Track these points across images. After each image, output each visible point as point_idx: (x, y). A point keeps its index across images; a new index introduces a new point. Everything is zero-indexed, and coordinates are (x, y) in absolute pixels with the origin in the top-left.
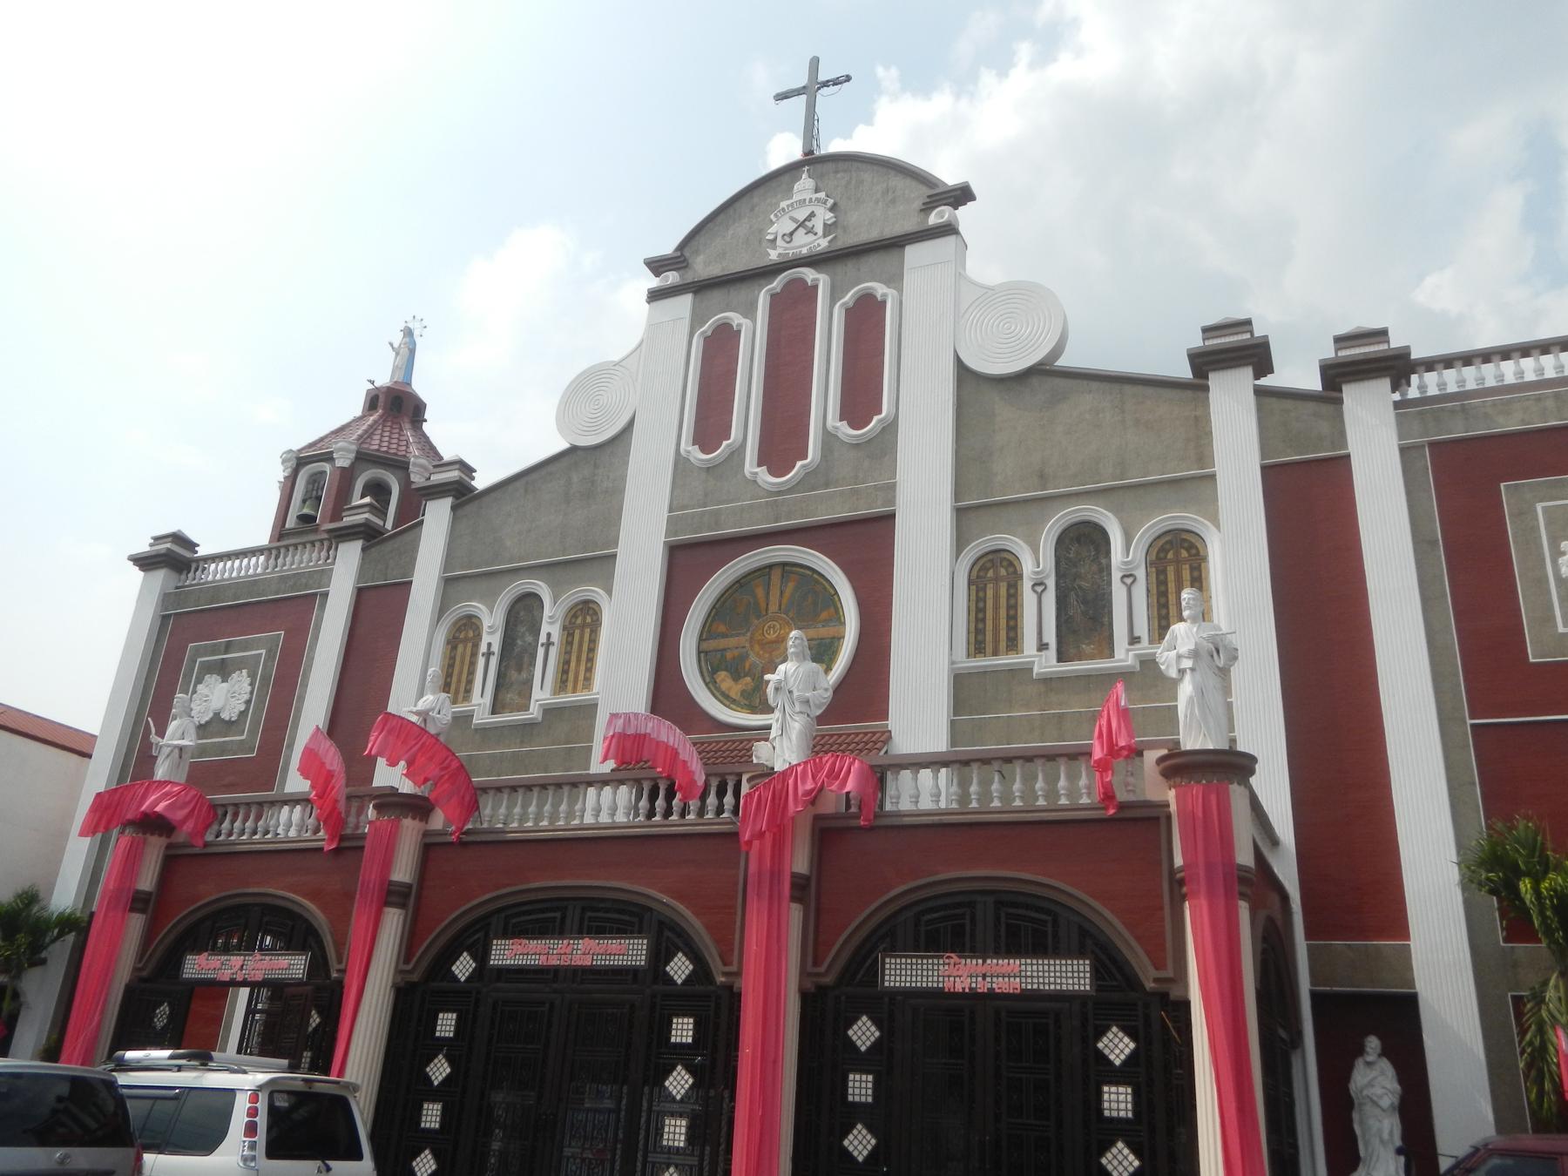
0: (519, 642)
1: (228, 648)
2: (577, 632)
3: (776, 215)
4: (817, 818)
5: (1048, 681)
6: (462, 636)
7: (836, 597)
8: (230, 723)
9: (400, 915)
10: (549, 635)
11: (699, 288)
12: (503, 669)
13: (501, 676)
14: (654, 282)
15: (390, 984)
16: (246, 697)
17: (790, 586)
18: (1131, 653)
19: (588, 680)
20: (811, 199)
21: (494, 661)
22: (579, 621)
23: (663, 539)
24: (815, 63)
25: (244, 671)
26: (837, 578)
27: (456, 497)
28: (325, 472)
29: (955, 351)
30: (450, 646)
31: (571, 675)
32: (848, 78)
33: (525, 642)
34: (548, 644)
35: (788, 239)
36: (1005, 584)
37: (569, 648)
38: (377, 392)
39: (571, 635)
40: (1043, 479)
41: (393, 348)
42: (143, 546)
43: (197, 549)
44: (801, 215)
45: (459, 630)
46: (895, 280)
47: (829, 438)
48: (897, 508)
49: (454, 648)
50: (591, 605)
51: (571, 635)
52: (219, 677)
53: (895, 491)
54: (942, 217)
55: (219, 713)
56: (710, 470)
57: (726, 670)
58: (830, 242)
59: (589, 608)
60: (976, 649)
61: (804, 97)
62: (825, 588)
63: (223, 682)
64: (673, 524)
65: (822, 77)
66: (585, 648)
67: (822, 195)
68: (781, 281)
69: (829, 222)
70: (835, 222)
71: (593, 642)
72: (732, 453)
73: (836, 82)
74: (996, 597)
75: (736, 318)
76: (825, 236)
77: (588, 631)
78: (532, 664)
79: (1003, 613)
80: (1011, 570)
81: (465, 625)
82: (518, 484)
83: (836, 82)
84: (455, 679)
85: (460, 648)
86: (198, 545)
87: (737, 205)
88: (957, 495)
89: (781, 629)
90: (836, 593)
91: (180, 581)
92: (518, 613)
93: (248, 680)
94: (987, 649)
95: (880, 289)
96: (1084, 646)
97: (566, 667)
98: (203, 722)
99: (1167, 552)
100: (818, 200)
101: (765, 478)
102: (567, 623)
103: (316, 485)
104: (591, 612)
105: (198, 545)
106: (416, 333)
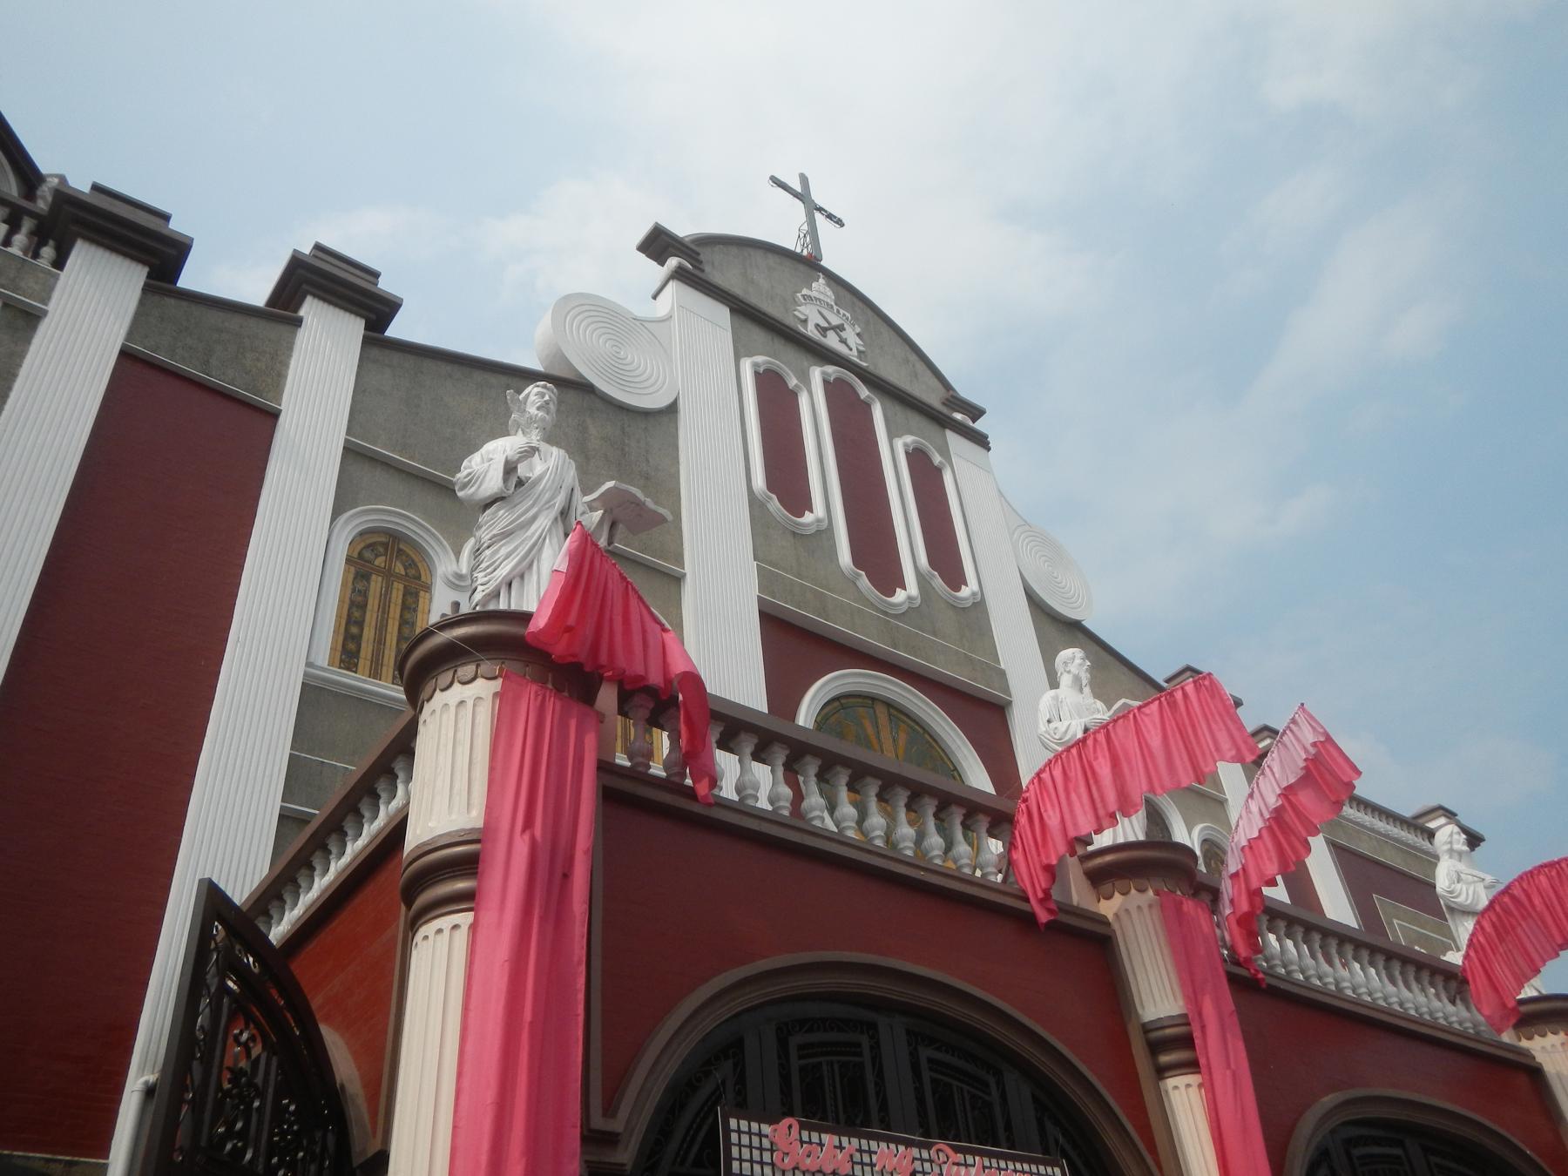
3: (805, 299)
11: (743, 311)
20: (838, 311)
24: (804, 180)
26: (966, 752)
30: (352, 569)
32: (840, 223)
44: (835, 321)
45: (371, 546)
46: (945, 453)
62: (942, 759)
67: (848, 315)
69: (862, 348)
72: (819, 532)
73: (830, 216)
81: (385, 545)
83: (830, 216)
84: (369, 633)
85: (376, 583)
99: (1210, 860)
100: (847, 319)
101: (864, 582)
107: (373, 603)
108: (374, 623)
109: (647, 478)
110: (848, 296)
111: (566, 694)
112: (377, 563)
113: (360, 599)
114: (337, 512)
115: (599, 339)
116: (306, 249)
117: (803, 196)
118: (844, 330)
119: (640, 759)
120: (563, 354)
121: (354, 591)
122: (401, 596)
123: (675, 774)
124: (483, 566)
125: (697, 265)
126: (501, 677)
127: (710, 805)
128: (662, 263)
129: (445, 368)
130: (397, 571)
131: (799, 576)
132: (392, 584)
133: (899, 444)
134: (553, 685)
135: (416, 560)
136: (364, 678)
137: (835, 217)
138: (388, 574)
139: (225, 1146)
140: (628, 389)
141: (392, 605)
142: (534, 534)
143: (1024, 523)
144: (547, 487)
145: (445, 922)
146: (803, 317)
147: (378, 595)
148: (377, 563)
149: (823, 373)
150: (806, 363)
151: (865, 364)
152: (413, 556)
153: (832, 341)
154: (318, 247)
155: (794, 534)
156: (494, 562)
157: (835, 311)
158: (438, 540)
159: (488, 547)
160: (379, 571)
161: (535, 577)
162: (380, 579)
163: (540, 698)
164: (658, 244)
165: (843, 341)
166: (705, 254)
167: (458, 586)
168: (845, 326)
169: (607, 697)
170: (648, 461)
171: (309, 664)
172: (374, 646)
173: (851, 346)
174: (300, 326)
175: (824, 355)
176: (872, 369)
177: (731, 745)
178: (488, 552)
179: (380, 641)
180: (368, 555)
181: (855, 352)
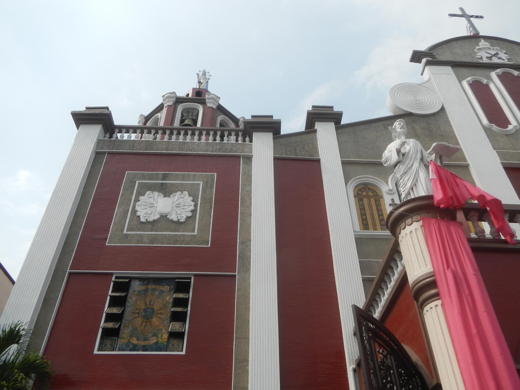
1: (165, 177)
3: (478, 50)
8: (178, 223)
11: (455, 65)
16: (192, 208)
20: (493, 49)
24: (462, 9)
25: (186, 193)
27: (335, 124)
30: (357, 199)
32: (482, 17)
35: (490, 59)
38: (199, 90)
41: (198, 77)
42: (81, 108)
44: (493, 52)
45: (360, 190)
52: (161, 194)
55: (167, 216)
63: (164, 197)
67: (498, 48)
69: (508, 58)
73: (477, 17)
81: (364, 188)
82: (378, 124)
83: (477, 17)
84: (369, 217)
85: (365, 201)
87: (451, 43)
91: (105, 137)
93: (191, 198)
98: (151, 219)
100: (498, 49)
103: (190, 114)
107: (367, 207)
108: (369, 213)
109: (442, 136)
110: (495, 41)
111: (446, 219)
112: (363, 194)
113: (362, 207)
114: (346, 183)
115: (408, 97)
116: (310, 109)
117: (464, 15)
118: (498, 54)
119: (481, 234)
120: (399, 107)
121: (359, 205)
122: (374, 202)
123: (496, 236)
124: (401, 185)
125: (433, 57)
126: (421, 220)
127: (515, 244)
128: (420, 63)
129: (362, 127)
130: (370, 195)
131: (514, 150)
132: (370, 199)
134: (440, 217)
135: (375, 189)
136: (372, 231)
137: (479, 16)
138: (368, 197)
139: (387, 386)
140: (424, 109)
141: (373, 206)
142: (414, 170)
144: (413, 153)
145: (432, 305)
146: (480, 57)
147: (367, 204)
148: (363, 194)
149: (496, 73)
150: (488, 73)
151: (512, 63)
152: (374, 189)
153: (495, 60)
154: (313, 107)
155: (507, 135)
156: (404, 183)
157: (492, 49)
158: (379, 181)
159: (401, 179)
160: (365, 197)
161: (420, 184)
163: (437, 223)
164: (416, 57)
165: (500, 58)
166: (435, 52)
167: (391, 193)
168: (498, 52)
169: (460, 216)
170: (440, 130)
171: (354, 232)
172: (372, 220)
173: (504, 59)
174: (317, 132)
175: (493, 67)
176: (516, 63)
177: (515, 220)
178: (401, 181)
179: (373, 218)
180: (360, 193)
181: (506, 60)
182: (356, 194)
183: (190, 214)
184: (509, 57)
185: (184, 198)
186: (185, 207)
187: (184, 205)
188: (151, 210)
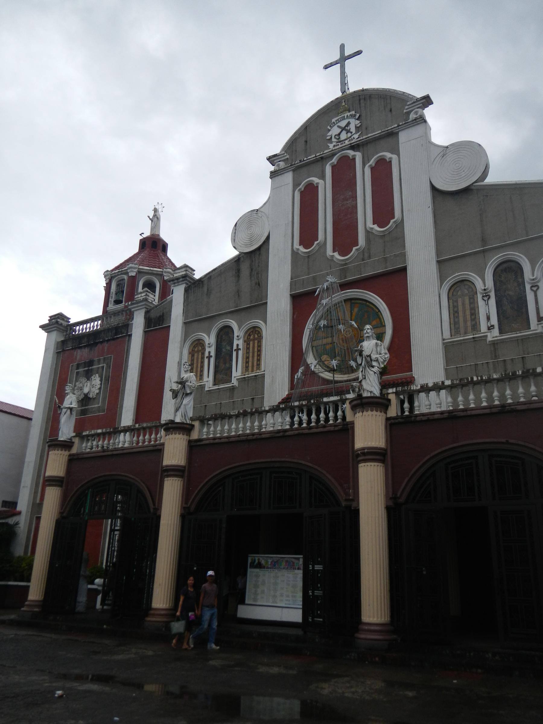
0: (224, 350)
2: (251, 343)
3: (330, 126)
4: (388, 419)
5: (494, 344)
6: (196, 349)
7: (379, 313)
9: (181, 481)
10: (238, 345)
12: (217, 364)
13: (216, 367)
14: (272, 168)
15: (179, 514)
16: (99, 386)
17: (356, 310)
18: (540, 326)
19: (259, 365)
20: (347, 115)
21: (212, 360)
22: (252, 337)
23: (289, 293)
24: (342, 47)
28: (125, 279)
29: (430, 182)
31: (250, 363)
33: (226, 350)
34: (238, 350)
35: (337, 137)
36: (468, 297)
37: (248, 351)
39: (248, 344)
40: (484, 241)
41: (150, 219)
43: (70, 320)
44: (343, 124)
45: (194, 347)
46: (396, 150)
47: (368, 233)
48: (407, 264)
49: (193, 356)
50: (257, 329)
51: (248, 344)
53: (405, 256)
54: (417, 114)
56: (309, 256)
57: (326, 355)
58: (359, 136)
59: (256, 331)
60: (455, 332)
61: (339, 65)
62: (373, 309)
64: (293, 284)
65: (347, 54)
66: (256, 350)
67: (353, 112)
68: (337, 158)
69: (358, 126)
70: (361, 125)
71: (260, 346)
72: (320, 247)
74: (463, 304)
75: (315, 180)
76: (356, 133)
77: (256, 341)
78: (231, 360)
79: (468, 312)
80: (470, 290)
81: (197, 344)
85: (196, 355)
86: (70, 319)
88: (438, 253)
89: (352, 331)
90: (379, 311)
92: (222, 336)
94: (461, 331)
95: (388, 155)
96: (513, 325)
97: (247, 360)
102: (246, 339)
104: (257, 332)
105: (70, 319)
106: (160, 210)
133: (367, 166)
140: (252, 244)
143: (442, 149)
146: (328, 138)
162: (196, 354)
165: (348, 131)
180: (193, 349)
182: (191, 351)
183: (98, 391)
184: (360, 123)
185: (96, 379)
186: (96, 387)
187: (96, 385)
188: (80, 393)
